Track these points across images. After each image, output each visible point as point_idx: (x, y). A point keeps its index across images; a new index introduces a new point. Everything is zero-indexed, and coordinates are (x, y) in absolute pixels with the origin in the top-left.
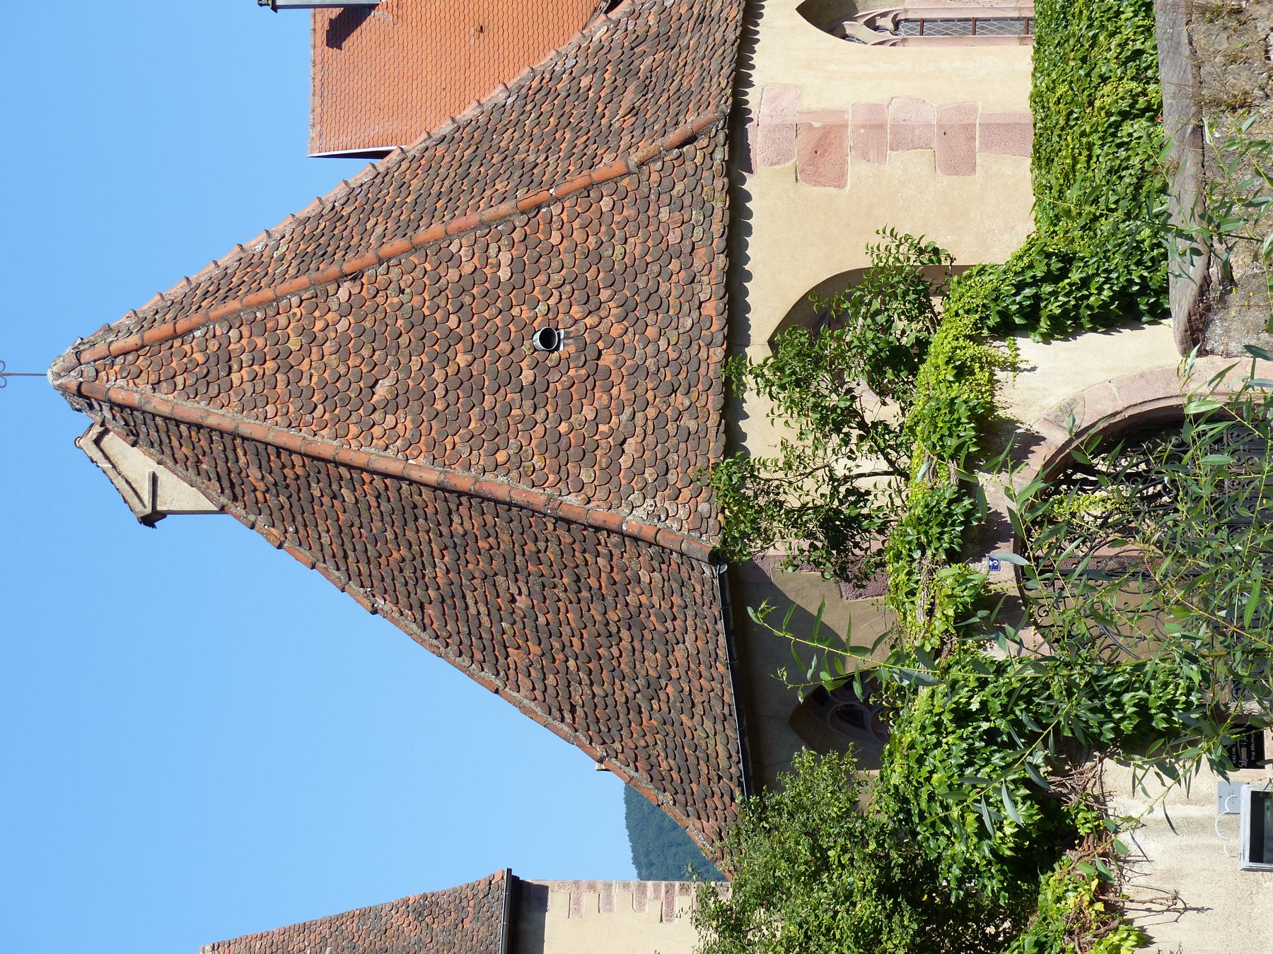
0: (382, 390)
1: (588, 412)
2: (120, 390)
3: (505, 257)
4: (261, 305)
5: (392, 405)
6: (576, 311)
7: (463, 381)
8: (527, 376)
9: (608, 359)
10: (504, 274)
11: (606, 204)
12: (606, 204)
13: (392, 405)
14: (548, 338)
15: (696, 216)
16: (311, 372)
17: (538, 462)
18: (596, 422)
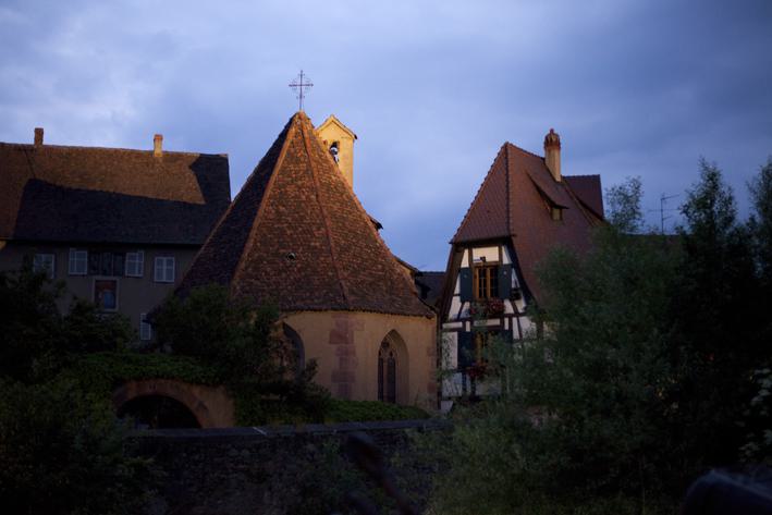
0: (282, 209)
1: (269, 269)
2: (293, 130)
3: (318, 244)
4: (312, 173)
5: (277, 212)
6: (299, 265)
7: (283, 232)
8: (282, 251)
9: (284, 275)
10: (313, 244)
11: (330, 274)
12: (330, 274)
13: (277, 212)
14: (291, 257)
15: (321, 300)
16: (290, 189)
17: (257, 255)
18: (266, 272)
